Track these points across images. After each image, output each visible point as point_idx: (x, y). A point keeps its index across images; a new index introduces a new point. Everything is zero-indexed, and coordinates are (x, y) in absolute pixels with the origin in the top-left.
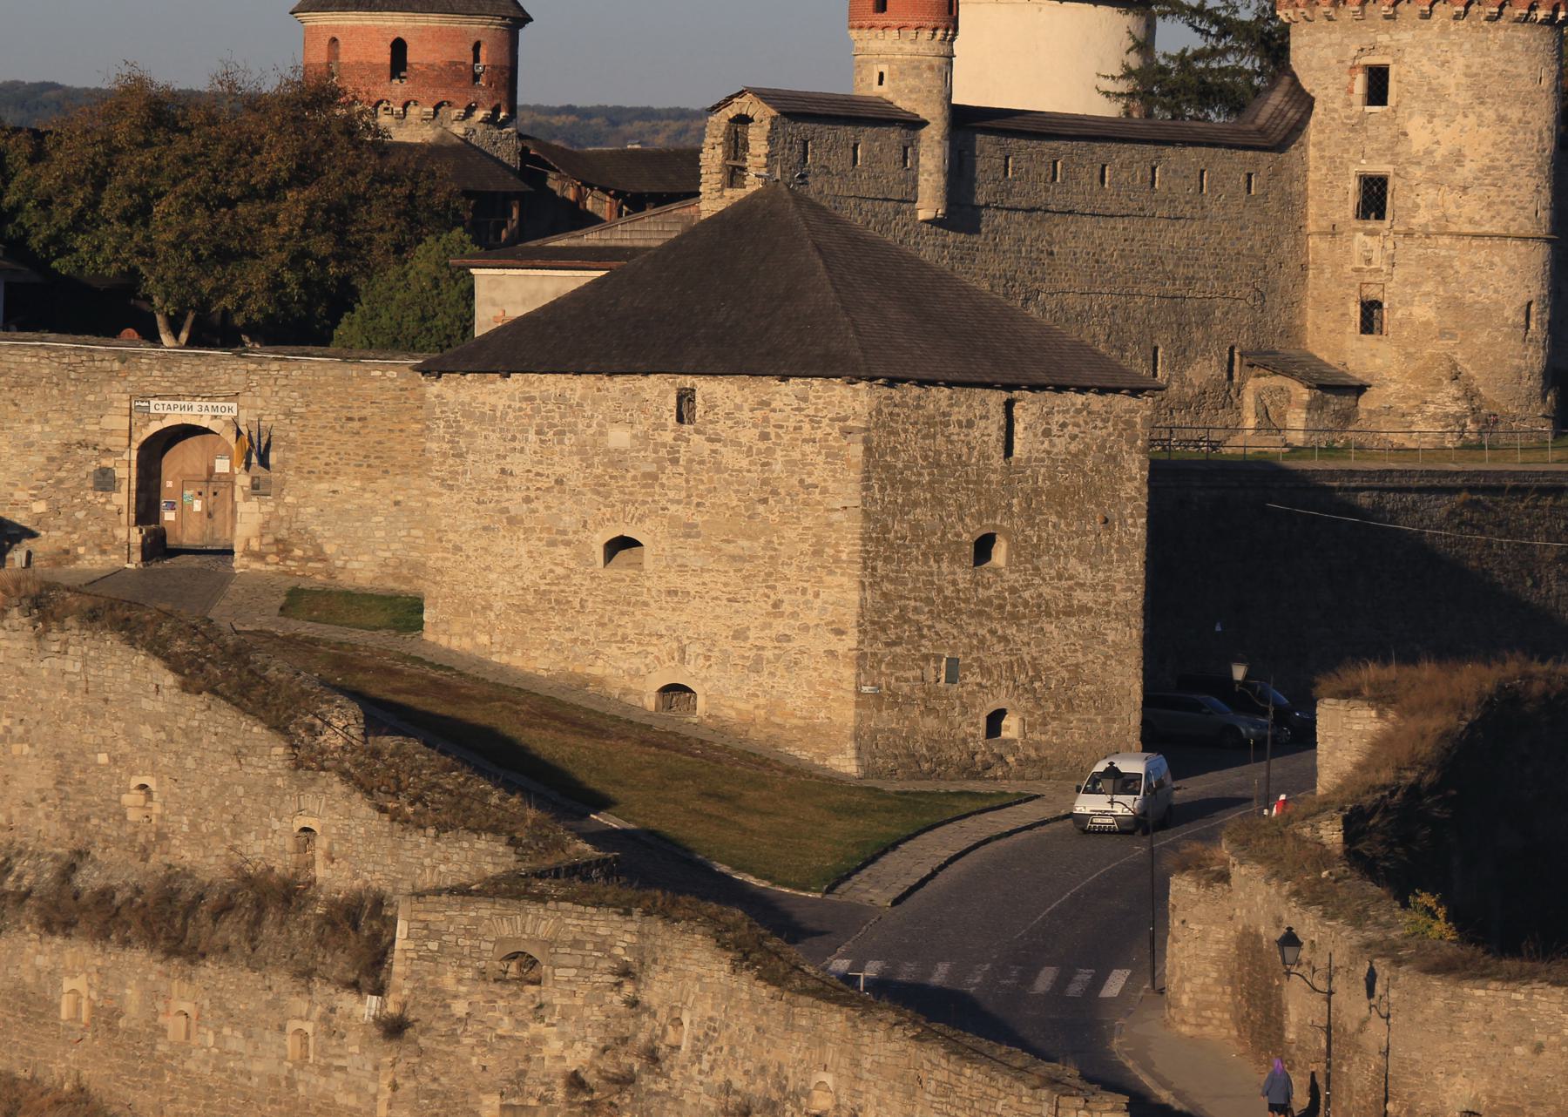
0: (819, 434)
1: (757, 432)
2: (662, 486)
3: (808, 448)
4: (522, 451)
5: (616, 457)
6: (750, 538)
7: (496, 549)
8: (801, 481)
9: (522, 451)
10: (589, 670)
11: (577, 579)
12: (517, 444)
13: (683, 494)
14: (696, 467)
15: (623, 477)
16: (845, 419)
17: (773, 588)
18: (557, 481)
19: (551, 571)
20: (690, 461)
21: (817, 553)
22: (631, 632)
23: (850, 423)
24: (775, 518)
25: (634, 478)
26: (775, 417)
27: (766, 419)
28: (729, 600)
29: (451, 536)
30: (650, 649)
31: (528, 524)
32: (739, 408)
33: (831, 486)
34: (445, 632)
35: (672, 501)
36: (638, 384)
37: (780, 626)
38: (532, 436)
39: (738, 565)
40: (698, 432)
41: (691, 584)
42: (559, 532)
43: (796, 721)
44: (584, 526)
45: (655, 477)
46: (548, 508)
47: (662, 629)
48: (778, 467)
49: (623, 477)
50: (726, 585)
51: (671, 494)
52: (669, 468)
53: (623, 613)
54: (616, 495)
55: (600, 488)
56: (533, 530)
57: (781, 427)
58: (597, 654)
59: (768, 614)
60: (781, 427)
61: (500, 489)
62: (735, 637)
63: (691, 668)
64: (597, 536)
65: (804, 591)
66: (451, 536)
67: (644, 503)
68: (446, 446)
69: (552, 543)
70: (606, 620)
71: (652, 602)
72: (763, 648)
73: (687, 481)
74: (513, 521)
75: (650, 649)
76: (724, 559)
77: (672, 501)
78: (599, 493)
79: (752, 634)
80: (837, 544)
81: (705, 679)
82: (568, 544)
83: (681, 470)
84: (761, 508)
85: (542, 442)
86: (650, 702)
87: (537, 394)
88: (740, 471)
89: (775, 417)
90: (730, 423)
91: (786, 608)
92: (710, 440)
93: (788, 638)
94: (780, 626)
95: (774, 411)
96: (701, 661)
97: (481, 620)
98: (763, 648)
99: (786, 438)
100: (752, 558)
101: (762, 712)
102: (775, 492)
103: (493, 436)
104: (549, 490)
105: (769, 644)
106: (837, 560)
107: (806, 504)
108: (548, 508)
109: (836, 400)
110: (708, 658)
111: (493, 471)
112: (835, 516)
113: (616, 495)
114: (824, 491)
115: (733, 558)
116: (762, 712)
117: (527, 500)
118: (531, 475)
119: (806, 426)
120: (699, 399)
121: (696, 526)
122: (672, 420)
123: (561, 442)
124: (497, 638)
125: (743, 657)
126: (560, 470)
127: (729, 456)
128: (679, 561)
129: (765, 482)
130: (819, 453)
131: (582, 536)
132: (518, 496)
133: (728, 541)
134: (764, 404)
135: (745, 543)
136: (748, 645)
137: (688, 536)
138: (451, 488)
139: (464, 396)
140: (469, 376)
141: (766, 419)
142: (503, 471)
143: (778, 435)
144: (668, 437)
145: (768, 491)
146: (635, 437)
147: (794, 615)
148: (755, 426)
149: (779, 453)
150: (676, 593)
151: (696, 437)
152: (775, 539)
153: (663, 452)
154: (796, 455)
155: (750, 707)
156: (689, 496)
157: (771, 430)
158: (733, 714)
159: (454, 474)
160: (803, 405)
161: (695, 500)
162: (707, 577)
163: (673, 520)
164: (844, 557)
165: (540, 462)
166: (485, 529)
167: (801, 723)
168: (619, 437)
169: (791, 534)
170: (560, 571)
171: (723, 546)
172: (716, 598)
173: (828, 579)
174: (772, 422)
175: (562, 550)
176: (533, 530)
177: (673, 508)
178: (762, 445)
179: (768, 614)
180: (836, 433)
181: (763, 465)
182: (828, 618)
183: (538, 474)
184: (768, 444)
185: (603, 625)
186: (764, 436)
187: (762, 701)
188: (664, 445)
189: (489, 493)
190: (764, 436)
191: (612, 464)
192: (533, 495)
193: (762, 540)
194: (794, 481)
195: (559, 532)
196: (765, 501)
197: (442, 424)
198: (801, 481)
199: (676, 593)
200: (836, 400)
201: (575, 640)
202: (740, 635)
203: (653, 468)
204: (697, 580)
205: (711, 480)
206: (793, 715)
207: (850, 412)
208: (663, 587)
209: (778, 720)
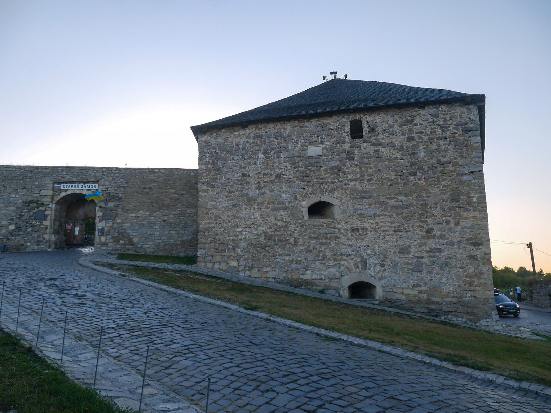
0: (448, 134)
1: (405, 137)
2: (344, 173)
3: (441, 142)
4: (255, 163)
5: (313, 160)
6: (406, 195)
7: (240, 215)
8: (439, 162)
9: (255, 163)
10: (302, 277)
11: (292, 227)
12: (252, 161)
13: (359, 175)
14: (366, 160)
15: (319, 170)
16: (466, 123)
17: (426, 222)
18: (277, 177)
19: (276, 224)
20: (362, 158)
21: (455, 198)
22: (329, 254)
23: (469, 125)
24: (422, 182)
25: (325, 170)
26: (416, 128)
27: (410, 130)
28: (395, 231)
29: (213, 211)
30: (342, 263)
31: (260, 200)
32: (392, 126)
33: (460, 161)
34: (210, 261)
35: (352, 180)
36: (325, 121)
37: (432, 244)
38: (261, 155)
39: (400, 210)
40: (365, 142)
41: (368, 224)
42: (279, 203)
43: (450, 299)
44: (296, 198)
45: (339, 169)
46: (272, 191)
47: (349, 250)
48: (422, 155)
49: (319, 170)
50: (391, 223)
51: (350, 177)
52: (348, 163)
53: (323, 244)
54: (314, 180)
55: (305, 177)
56: (263, 203)
57: (422, 133)
58: (306, 269)
59: (423, 237)
60: (422, 133)
61: (242, 184)
62: (400, 253)
63: (371, 272)
64: (304, 203)
65: (448, 222)
66: (213, 211)
67: (333, 183)
68: (210, 166)
69: (277, 210)
70: (312, 248)
71: (341, 236)
72: (422, 257)
73: (360, 168)
74: (251, 200)
75: (342, 263)
76: (389, 208)
77: (352, 180)
78: (304, 181)
79: (413, 250)
80: (469, 193)
81: (381, 279)
82: (285, 209)
83: (356, 163)
84: (412, 178)
85: (267, 158)
86: (345, 293)
87: (264, 134)
88: (396, 158)
89: (416, 128)
90: (386, 135)
91: (437, 233)
92: (374, 145)
93: (440, 251)
94: (432, 244)
95: (416, 125)
96: (378, 268)
97: (232, 254)
98: (422, 257)
99: (425, 139)
100: (408, 207)
101: (425, 295)
102: (421, 169)
103: (237, 158)
104: (272, 182)
105: (425, 255)
106: (470, 203)
107: (443, 173)
108: (272, 191)
109: (457, 115)
110: (382, 266)
111: (238, 176)
112: (465, 178)
113: (314, 180)
114: (456, 165)
115: (395, 207)
116: (425, 295)
117: (259, 188)
118: (260, 176)
119: (439, 131)
120: (365, 125)
121: (369, 192)
122: (348, 138)
123: (278, 157)
124: (242, 262)
125: (408, 263)
126: (278, 171)
127: (386, 152)
128: (359, 212)
129: (412, 164)
130: (450, 144)
131: (294, 203)
132: (253, 187)
133: (391, 199)
134: (411, 122)
135: (404, 198)
136: (411, 256)
137: (364, 198)
138: (213, 186)
139: (220, 140)
140: (223, 130)
141: (410, 130)
142: (244, 175)
143: (419, 138)
144: (347, 146)
145: (416, 167)
146: (323, 149)
147: (442, 237)
148: (403, 134)
149: (421, 147)
150: (358, 230)
151: (365, 144)
152: (424, 194)
153: (344, 155)
154: (434, 146)
155: (415, 292)
156: (362, 176)
157: (416, 136)
158: (404, 297)
159: (215, 180)
160: (435, 119)
161: (367, 178)
162: (378, 220)
163: (353, 191)
164: (475, 200)
165: (267, 168)
166: (234, 205)
167: (455, 300)
168: (315, 150)
169: (435, 190)
170: (280, 223)
171: (388, 201)
172: (386, 231)
173: (464, 214)
174: (415, 131)
175: (282, 213)
176: (263, 203)
177: (352, 184)
178: (410, 144)
179: (423, 237)
180: (460, 131)
181: (412, 154)
182: (467, 236)
183: (265, 174)
184: (414, 143)
185: (310, 251)
186: (410, 139)
187: (424, 288)
188: (344, 151)
189: (236, 187)
190: (410, 139)
191: (312, 164)
192: (262, 185)
193: (415, 195)
194: (433, 161)
195: (279, 203)
196: (415, 174)
197: (208, 155)
198: (439, 162)
199: (358, 230)
200: (457, 115)
201: (292, 261)
202: (404, 250)
203: (338, 163)
204: (371, 221)
205: (376, 166)
206: (448, 296)
207: (468, 119)
208: (349, 227)
209: (437, 299)
